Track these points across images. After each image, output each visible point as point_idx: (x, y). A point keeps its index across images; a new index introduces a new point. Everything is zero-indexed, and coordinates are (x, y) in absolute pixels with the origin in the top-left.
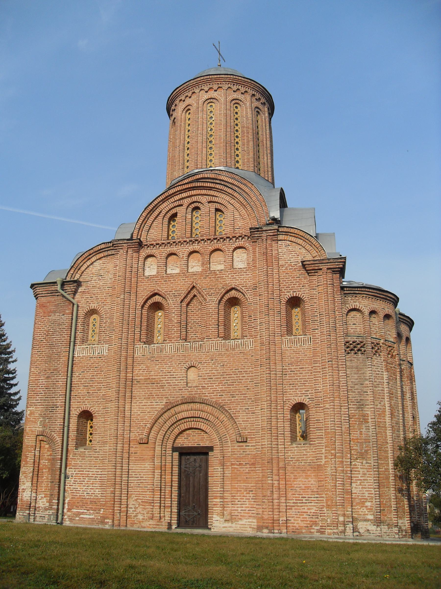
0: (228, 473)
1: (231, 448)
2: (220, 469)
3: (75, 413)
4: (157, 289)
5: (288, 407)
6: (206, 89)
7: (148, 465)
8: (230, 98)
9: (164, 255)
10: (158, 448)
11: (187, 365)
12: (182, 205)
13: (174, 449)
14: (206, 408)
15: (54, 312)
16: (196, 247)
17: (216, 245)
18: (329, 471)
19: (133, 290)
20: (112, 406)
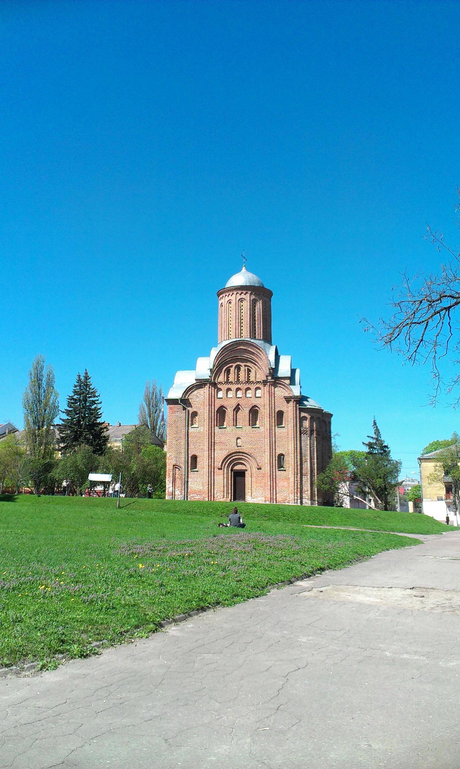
0: (254, 480)
1: (255, 470)
2: (250, 478)
3: (190, 456)
4: (223, 404)
5: (277, 455)
6: (240, 292)
7: (222, 477)
8: (252, 298)
9: (226, 389)
10: (225, 470)
11: (236, 437)
12: (232, 366)
13: (232, 470)
14: (244, 455)
15: (177, 412)
16: (239, 386)
17: (248, 386)
18: (292, 480)
19: (213, 404)
20: (206, 453)
